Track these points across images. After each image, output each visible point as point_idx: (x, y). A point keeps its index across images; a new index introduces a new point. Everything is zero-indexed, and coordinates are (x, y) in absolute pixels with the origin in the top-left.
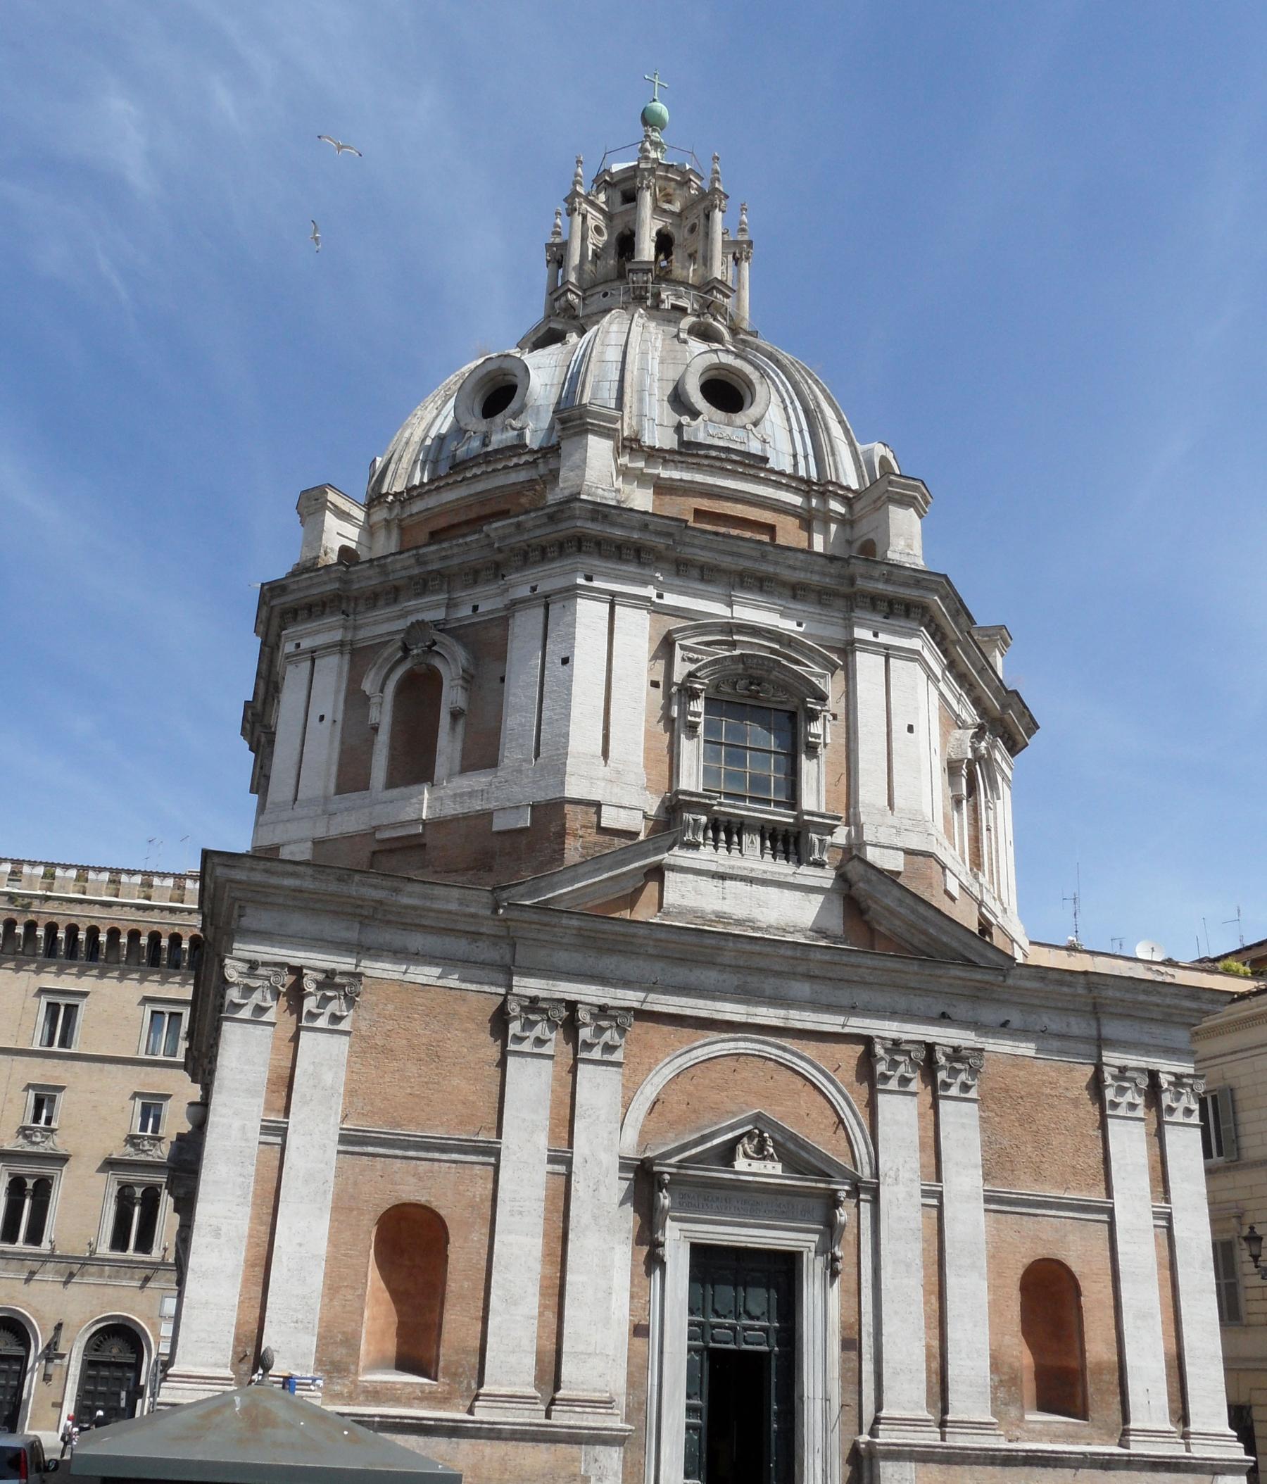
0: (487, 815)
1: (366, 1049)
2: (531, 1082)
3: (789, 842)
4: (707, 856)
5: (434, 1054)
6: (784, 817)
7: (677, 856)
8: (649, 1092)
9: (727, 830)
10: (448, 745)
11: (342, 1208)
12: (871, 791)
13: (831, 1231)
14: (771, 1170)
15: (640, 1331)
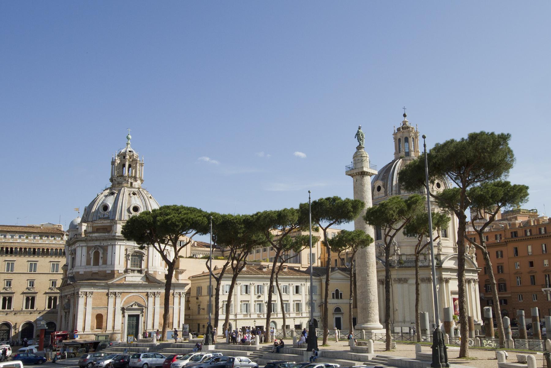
0: (106, 271)
1: (94, 299)
2: (111, 300)
3: (140, 272)
4: (131, 274)
5: (101, 299)
6: (139, 269)
7: (128, 275)
8: (124, 300)
9: (133, 271)
10: (101, 261)
11: (92, 315)
12: (150, 264)
13: (142, 312)
14: (137, 307)
15: (123, 323)
